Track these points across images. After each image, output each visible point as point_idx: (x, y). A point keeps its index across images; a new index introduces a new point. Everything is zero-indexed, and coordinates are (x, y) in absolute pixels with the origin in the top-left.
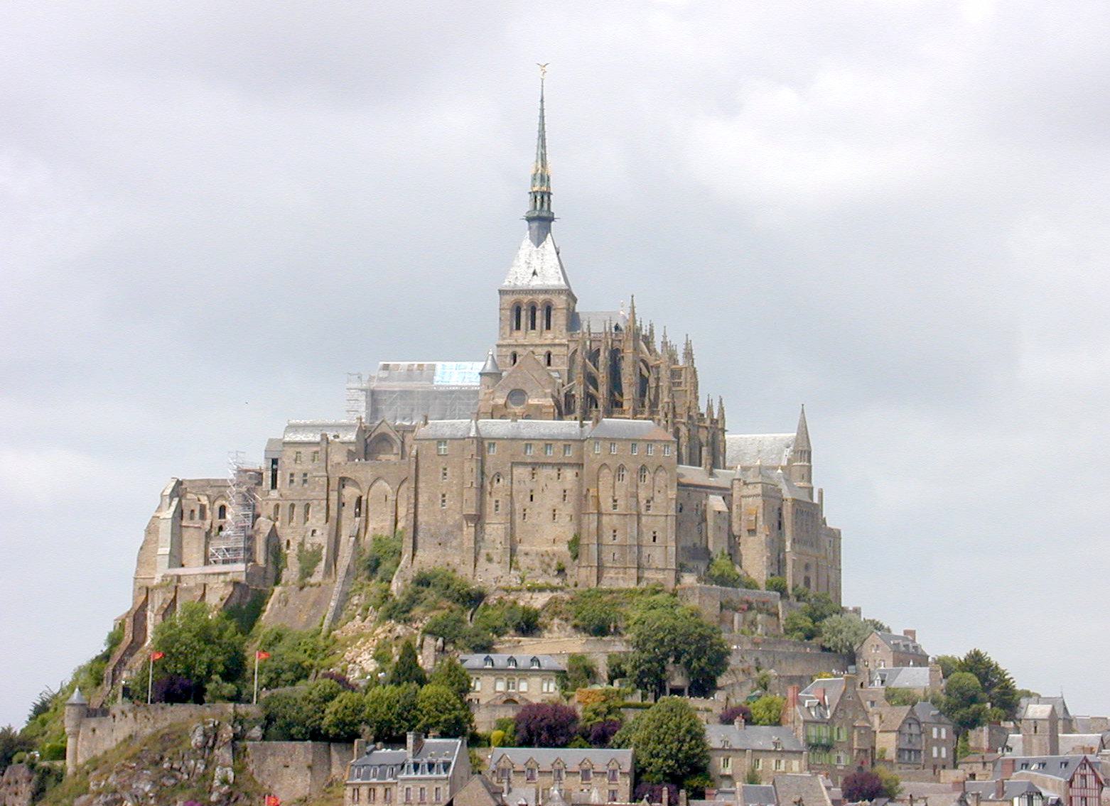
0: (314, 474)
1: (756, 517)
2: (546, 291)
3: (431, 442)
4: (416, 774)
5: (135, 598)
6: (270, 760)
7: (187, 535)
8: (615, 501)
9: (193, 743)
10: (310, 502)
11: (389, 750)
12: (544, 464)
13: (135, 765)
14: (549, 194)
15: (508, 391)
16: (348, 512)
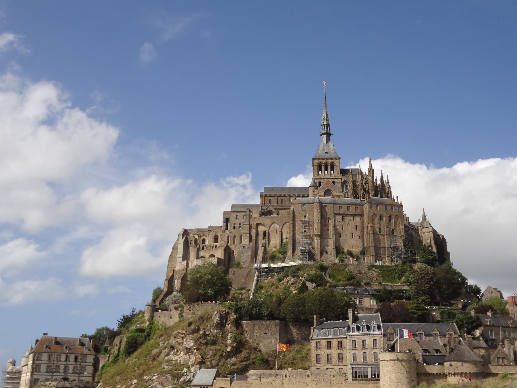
0: (244, 224)
1: (431, 241)
2: (332, 159)
3: (299, 205)
4: (358, 332)
5: (167, 275)
6: (256, 330)
7: (191, 249)
8: (380, 229)
9: (215, 322)
10: (242, 235)
11: (333, 321)
12: (347, 215)
13: (184, 332)
14: (329, 125)
15: (324, 191)
16: (260, 237)
